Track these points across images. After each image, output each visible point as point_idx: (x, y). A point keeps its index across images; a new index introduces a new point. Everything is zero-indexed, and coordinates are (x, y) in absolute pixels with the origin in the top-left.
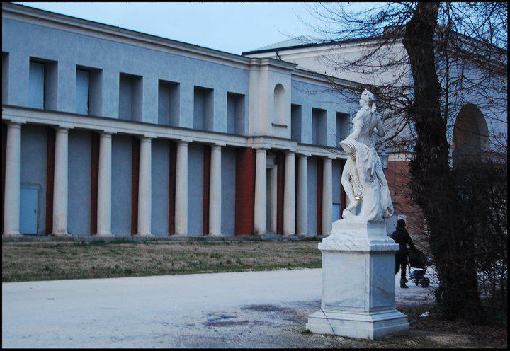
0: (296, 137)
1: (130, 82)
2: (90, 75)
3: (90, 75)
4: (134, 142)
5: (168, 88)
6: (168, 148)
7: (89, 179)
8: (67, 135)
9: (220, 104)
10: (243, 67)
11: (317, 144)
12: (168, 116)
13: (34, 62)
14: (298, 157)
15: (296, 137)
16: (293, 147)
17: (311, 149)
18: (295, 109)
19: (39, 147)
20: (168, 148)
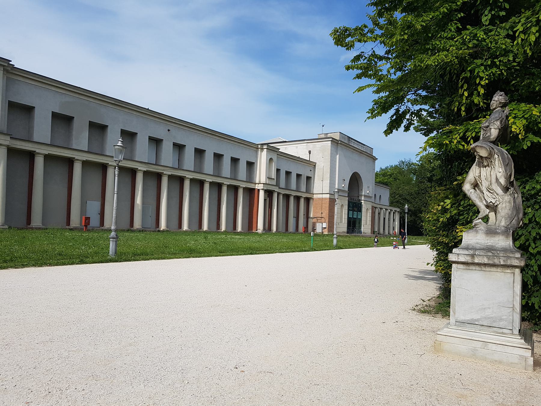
0: (278, 185)
1: (199, 153)
2: (179, 148)
3: (179, 148)
4: (219, 186)
5: (199, 153)
6: (217, 187)
7: (178, 201)
8: (81, 164)
9: (242, 166)
10: (254, 149)
11: (298, 190)
12: (217, 172)
13: (175, 145)
14: (279, 194)
15: (278, 185)
16: (276, 189)
17: (284, 190)
18: (278, 170)
19: (153, 183)
20: (234, 189)
